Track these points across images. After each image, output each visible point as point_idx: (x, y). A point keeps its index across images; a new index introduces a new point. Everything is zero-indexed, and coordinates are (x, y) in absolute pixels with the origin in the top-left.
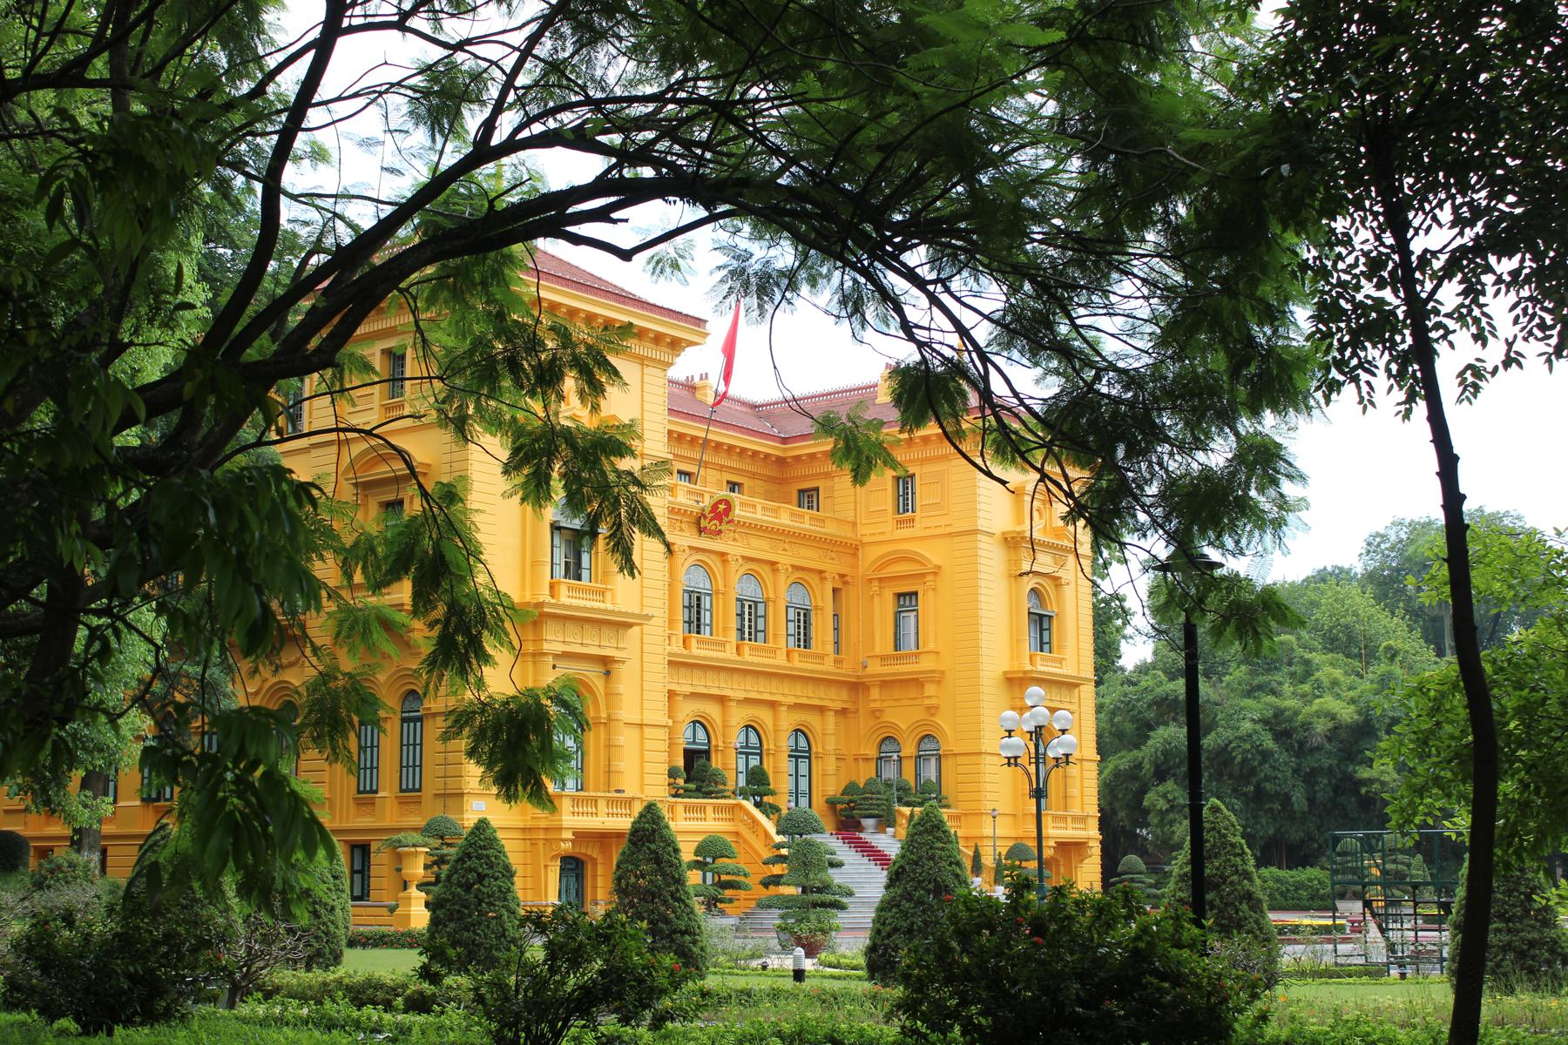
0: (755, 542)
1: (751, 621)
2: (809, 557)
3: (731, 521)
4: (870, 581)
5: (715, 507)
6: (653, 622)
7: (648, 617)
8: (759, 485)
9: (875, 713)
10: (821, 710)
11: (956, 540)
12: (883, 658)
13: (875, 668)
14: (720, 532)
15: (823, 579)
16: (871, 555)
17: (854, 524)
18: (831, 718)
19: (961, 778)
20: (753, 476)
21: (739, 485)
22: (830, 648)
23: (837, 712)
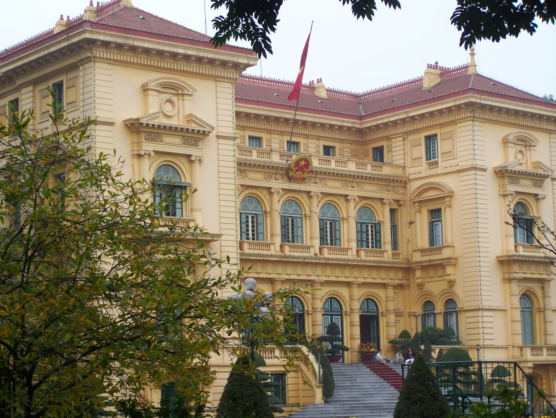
0: (330, 183)
1: (329, 233)
2: (370, 190)
3: (312, 172)
4: (414, 203)
5: (297, 163)
6: (222, 238)
7: (219, 236)
8: (347, 149)
9: (420, 286)
10: (384, 286)
11: (462, 174)
12: (423, 251)
13: (417, 257)
14: (303, 179)
15: (383, 204)
16: (414, 185)
17: (404, 167)
18: (391, 292)
19: (469, 326)
20: (342, 141)
21: (333, 148)
22: (388, 247)
23: (396, 287)
